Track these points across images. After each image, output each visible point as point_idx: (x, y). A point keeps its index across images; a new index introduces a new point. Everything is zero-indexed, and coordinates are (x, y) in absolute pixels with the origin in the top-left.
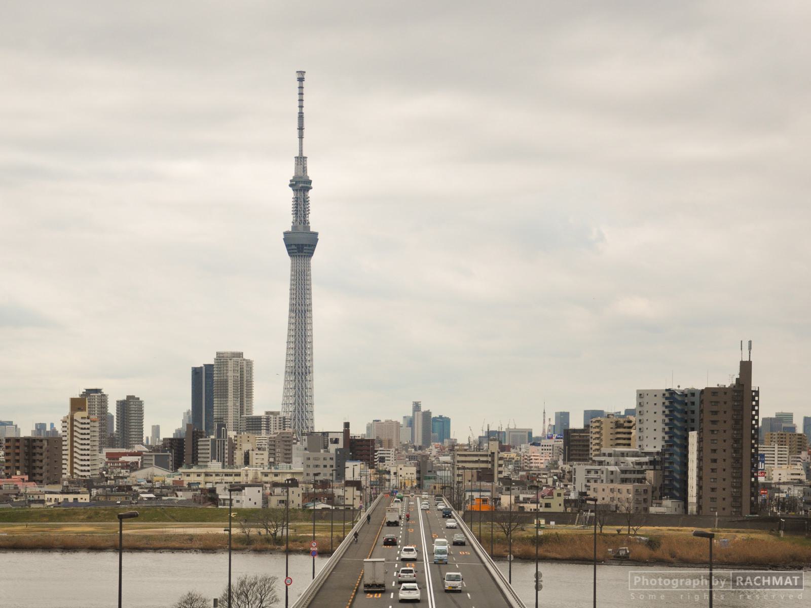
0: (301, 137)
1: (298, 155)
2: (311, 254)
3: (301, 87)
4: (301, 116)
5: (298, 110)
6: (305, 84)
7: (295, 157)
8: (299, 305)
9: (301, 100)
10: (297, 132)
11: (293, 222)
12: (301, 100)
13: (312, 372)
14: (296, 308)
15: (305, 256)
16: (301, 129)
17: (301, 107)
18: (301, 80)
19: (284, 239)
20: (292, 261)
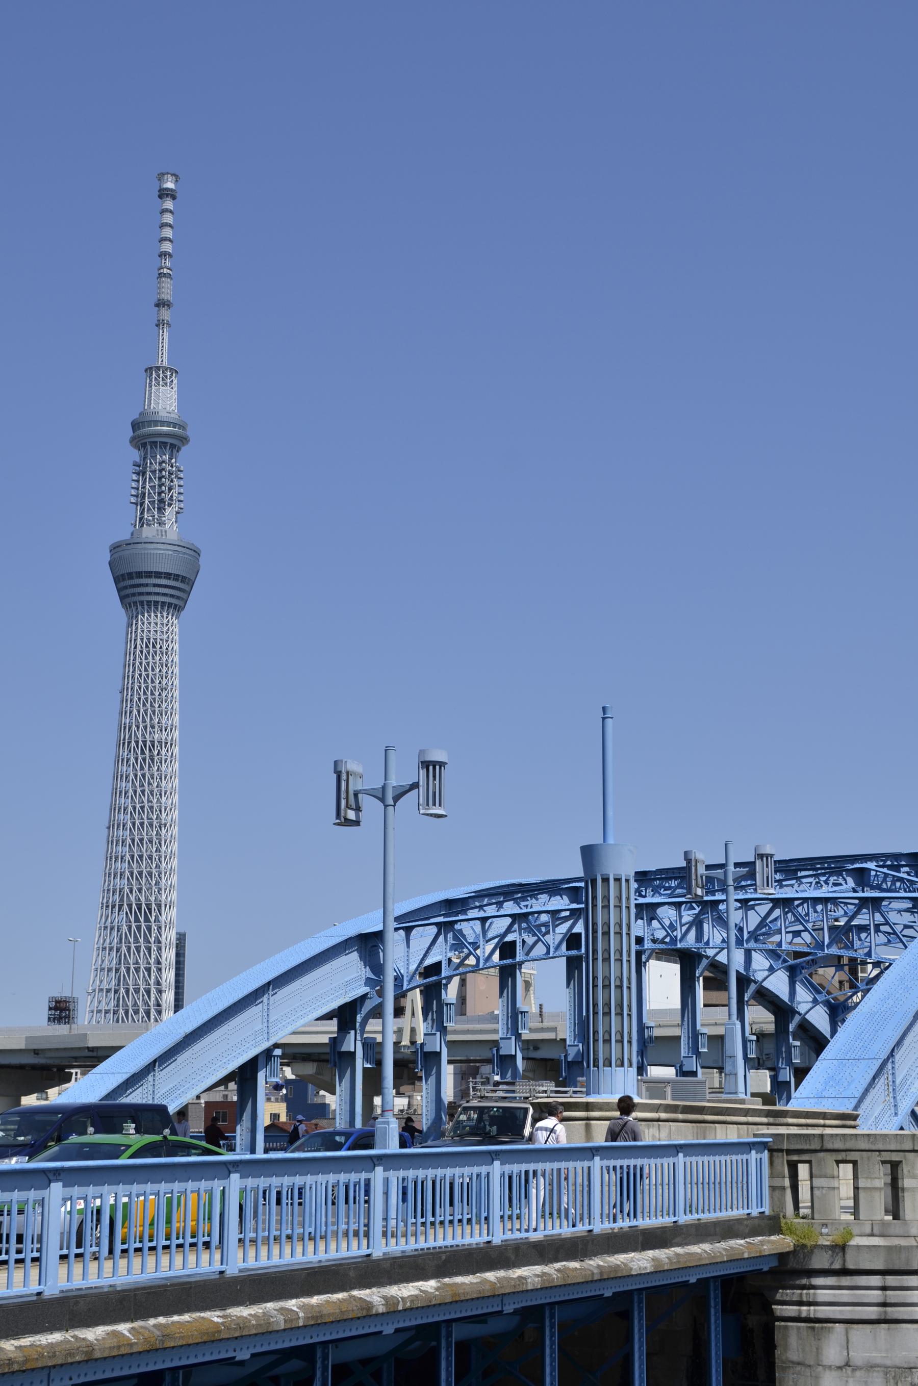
14: (130, 737)
19: (110, 564)
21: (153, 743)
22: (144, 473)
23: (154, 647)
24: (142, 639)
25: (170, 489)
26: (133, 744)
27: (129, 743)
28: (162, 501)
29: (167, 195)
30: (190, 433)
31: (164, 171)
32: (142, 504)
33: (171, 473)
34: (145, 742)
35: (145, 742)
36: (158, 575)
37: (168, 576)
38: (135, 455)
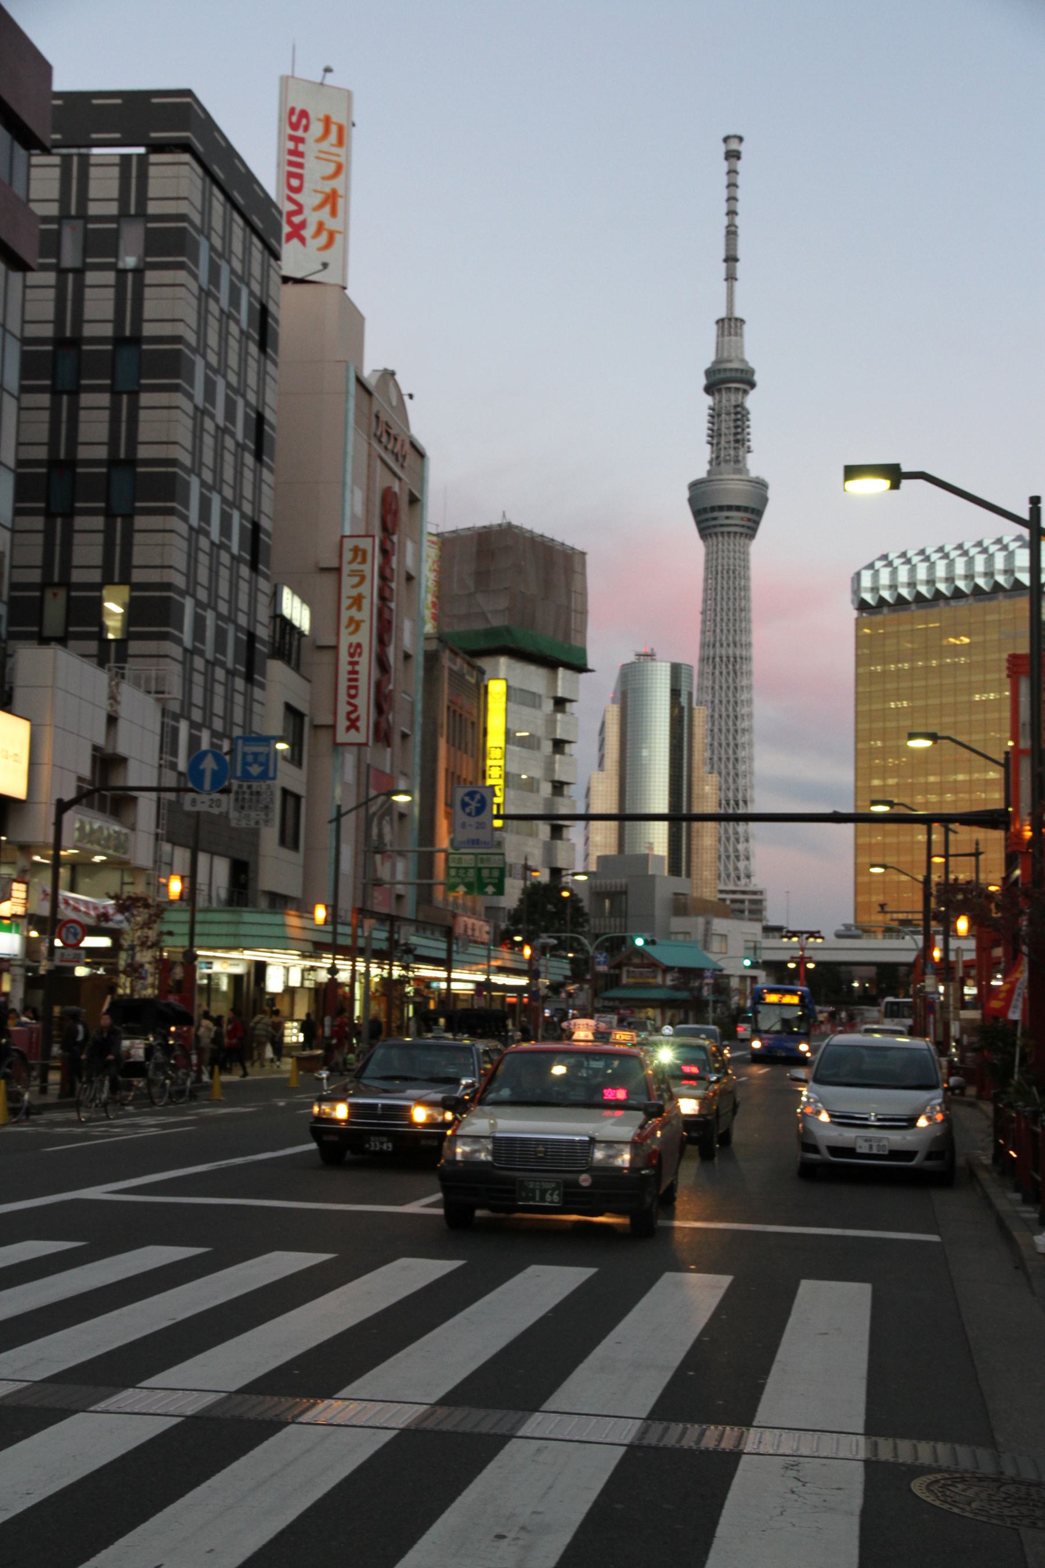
0: (731, 277)
1: (722, 314)
2: (751, 530)
3: (732, 172)
4: (731, 233)
5: (725, 221)
6: (740, 165)
7: (717, 322)
8: (721, 645)
9: (732, 199)
10: (721, 269)
11: (711, 462)
12: (732, 199)
13: (752, 801)
15: (735, 533)
16: (731, 259)
17: (732, 213)
18: (733, 155)
20: (707, 547)
21: (735, 658)
22: (719, 415)
23: (734, 572)
24: (723, 566)
25: (743, 430)
26: (717, 659)
27: (714, 658)
28: (737, 441)
29: (733, 156)
30: (757, 378)
31: (732, 133)
32: (718, 443)
33: (743, 416)
34: (728, 657)
35: (728, 657)
36: (738, 508)
37: (746, 509)
38: (709, 400)
